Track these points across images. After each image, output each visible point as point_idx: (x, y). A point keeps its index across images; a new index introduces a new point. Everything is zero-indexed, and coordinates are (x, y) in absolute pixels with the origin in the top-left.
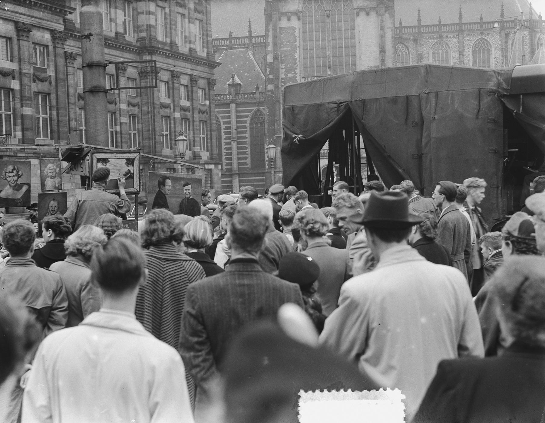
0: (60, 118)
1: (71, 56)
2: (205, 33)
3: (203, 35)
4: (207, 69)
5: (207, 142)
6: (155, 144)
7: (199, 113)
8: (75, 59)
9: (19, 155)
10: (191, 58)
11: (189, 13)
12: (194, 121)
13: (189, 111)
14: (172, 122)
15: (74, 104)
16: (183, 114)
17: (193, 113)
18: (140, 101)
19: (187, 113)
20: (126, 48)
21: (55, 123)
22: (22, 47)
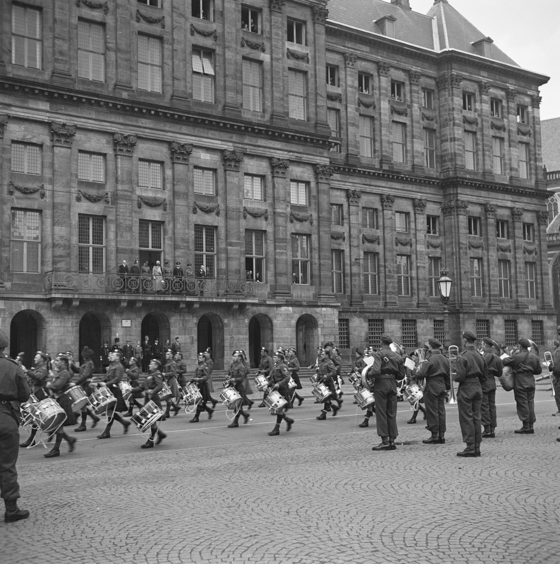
0: (322, 261)
1: (354, 194)
2: (533, 157)
3: (530, 160)
4: (535, 201)
5: (537, 288)
6: (461, 290)
7: (524, 253)
8: (359, 197)
9: (268, 303)
10: (513, 189)
11: (509, 136)
12: (516, 263)
13: (510, 251)
14: (485, 264)
15: (358, 246)
16: (501, 255)
17: (515, 253)
18: (443, 241)
19: (508, 254)
20: (425, 181)
21: (316, 267)
22: (276, 185)
